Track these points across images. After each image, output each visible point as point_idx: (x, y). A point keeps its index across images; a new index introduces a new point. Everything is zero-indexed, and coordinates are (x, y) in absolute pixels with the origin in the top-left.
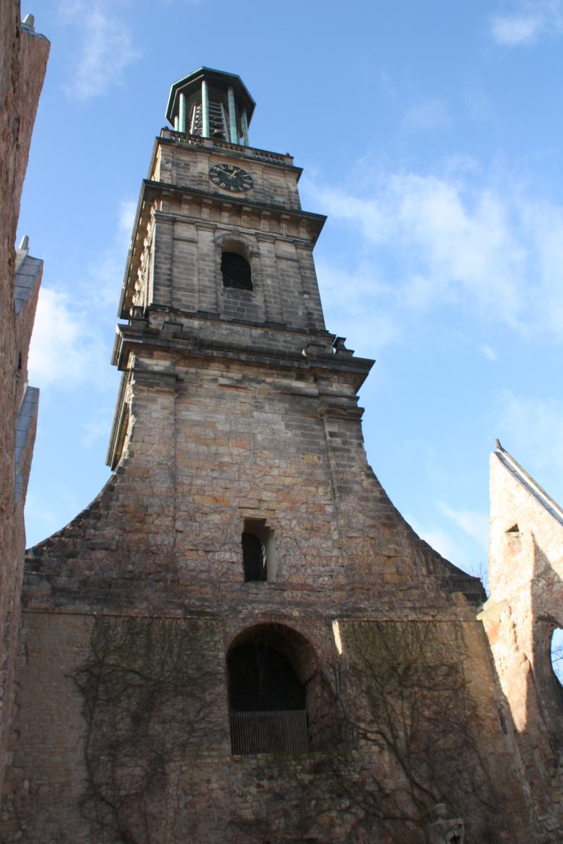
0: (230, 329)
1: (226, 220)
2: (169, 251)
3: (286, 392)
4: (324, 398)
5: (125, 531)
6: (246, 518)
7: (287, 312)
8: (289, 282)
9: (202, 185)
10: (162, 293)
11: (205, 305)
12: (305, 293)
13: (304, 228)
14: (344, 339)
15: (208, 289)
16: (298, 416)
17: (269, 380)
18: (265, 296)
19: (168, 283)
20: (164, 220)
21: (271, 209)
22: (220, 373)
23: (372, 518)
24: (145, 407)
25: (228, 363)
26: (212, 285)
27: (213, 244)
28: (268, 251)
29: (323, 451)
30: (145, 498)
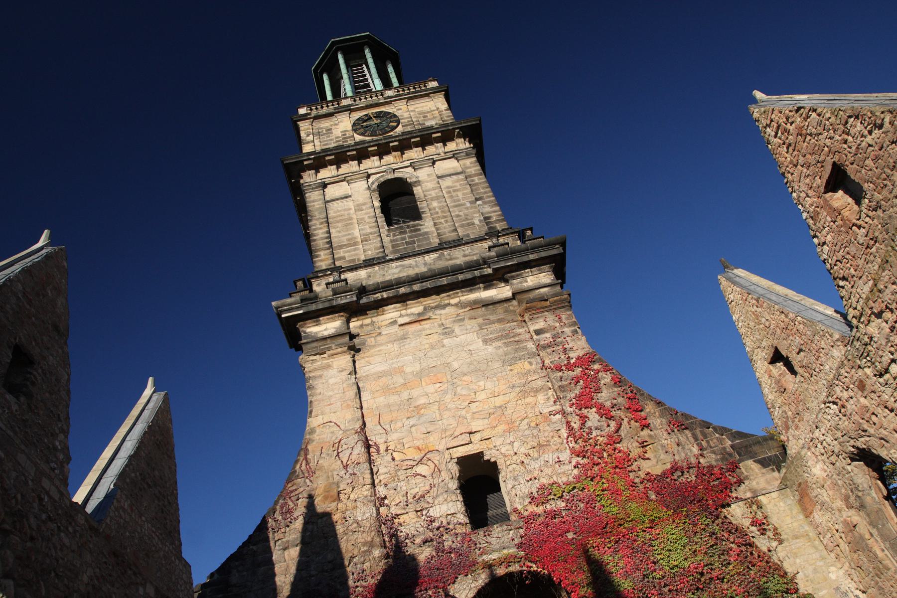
0: (401, 266)
1: (377, 163)
4: (518, 297)
8: (457, 196)
10: (323, 257)
11: (370, 252)
12: (477, 199)
15: (371, 236)
17: (454, 301)
18: (433, 219)
24: (321, 376)
26: (376, 230)
27: (368, 192)
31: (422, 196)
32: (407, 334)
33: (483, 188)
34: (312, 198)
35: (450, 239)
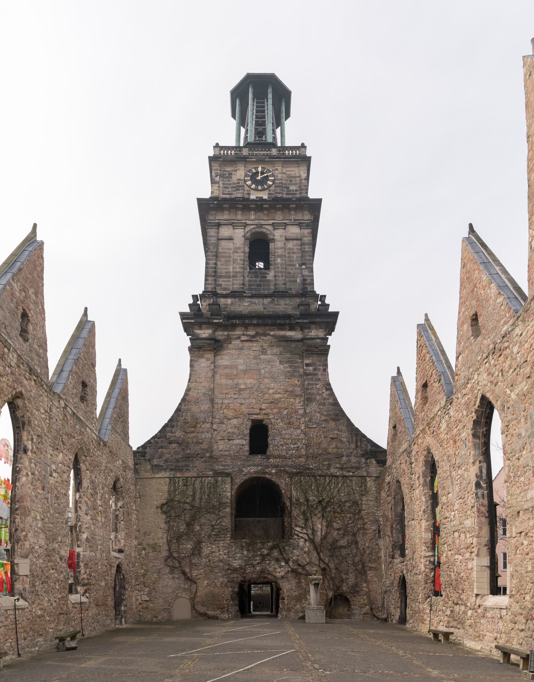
0: (250, 301)
1: (253, 217)
2: (215, 250)
3: (282, 340)
4: (305, 341)
5: (186, 432)
6: (253, 421)
7: (290, 281)
8: (293, 257)
9: (238, 190)
10: (210, 282)
11: (236, 286)
12: (303, 264)
14: (325, 296)
15: (239, 274)
16: (288, 355)
17: (272, 333)
18: (275, 272)
20: (212, 226)
23: (326, 416)
25: (246, 327)
26: (242, 270)
27: (243, 239)
28: (281, 236)
29: (301, 376)
32: (243, 346)
34: (211, 234)
35: (281, 290)
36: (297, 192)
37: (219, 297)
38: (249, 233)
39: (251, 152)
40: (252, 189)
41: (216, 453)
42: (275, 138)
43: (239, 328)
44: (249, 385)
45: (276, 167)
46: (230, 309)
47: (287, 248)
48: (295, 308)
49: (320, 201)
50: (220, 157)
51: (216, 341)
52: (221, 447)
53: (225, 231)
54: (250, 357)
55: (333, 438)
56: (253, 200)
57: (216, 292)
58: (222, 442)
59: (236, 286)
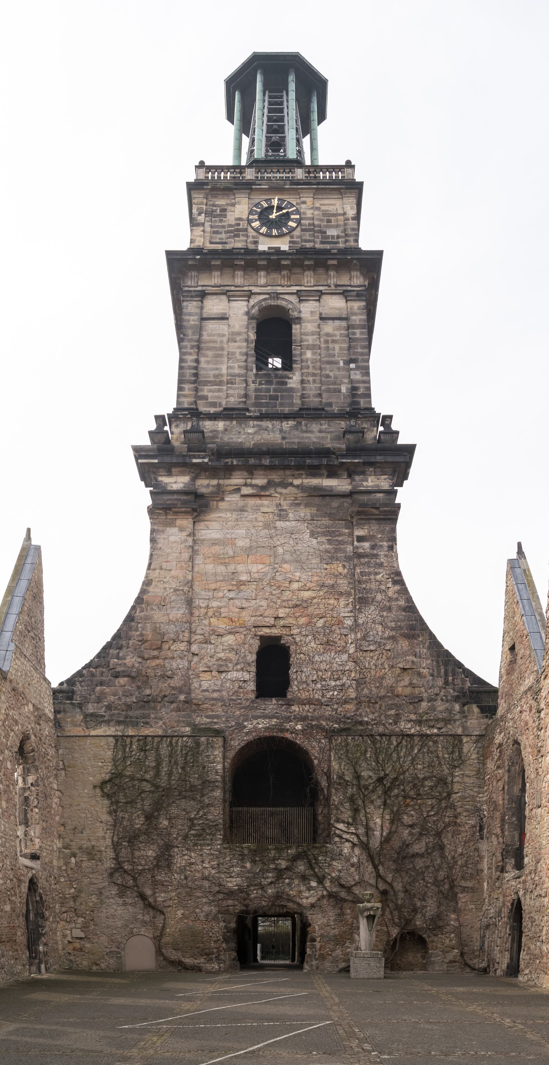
1: (262, 281)
2: (196, 337)
3: (315, 494)
4: (355, 496)
5: (143, 658)
6: (262, 638)
7: (328, 391)
9: (238, 236)
10: (186, 392)
11: (232, 399)
13: (356, 270)
14: (390, 417)
15: (237, 379)
16: (326, 521)
17: (297, 482)
18: (302, 374)
19: (193, 378)
20: (192, 297)
21: (314, 257)
22: (244, 480)
23: (392, 629)
25: (251, 470)
26: (243, 372)
27: (246, 318)
28: (312, 312)
29: (349, 559)
30: (162, 625)
31: (299, 339)
32: (246, 506)
33: (362, 347)
35: (312, 406)
36: (340, 240)
37: (203, 419)
38: (257, 308)
39: (259, 175)
40: (262, 234)
41: (197, 695)
42: (300, 152)
43: (237, 473)
44: (256, 575)
45: (302, 199)
46: (221, 439)
47: (322, 333)
48: (337, 438)
49: (380, 254)
50: (207, 184)
51: (197, 496)
52: (205, 685)
53: (214, 305)
54: (257, 524)
55: (405, 669)
56: (264, 253)
57: (197, 409)
58: (207, 676)
59: (232, 399)
